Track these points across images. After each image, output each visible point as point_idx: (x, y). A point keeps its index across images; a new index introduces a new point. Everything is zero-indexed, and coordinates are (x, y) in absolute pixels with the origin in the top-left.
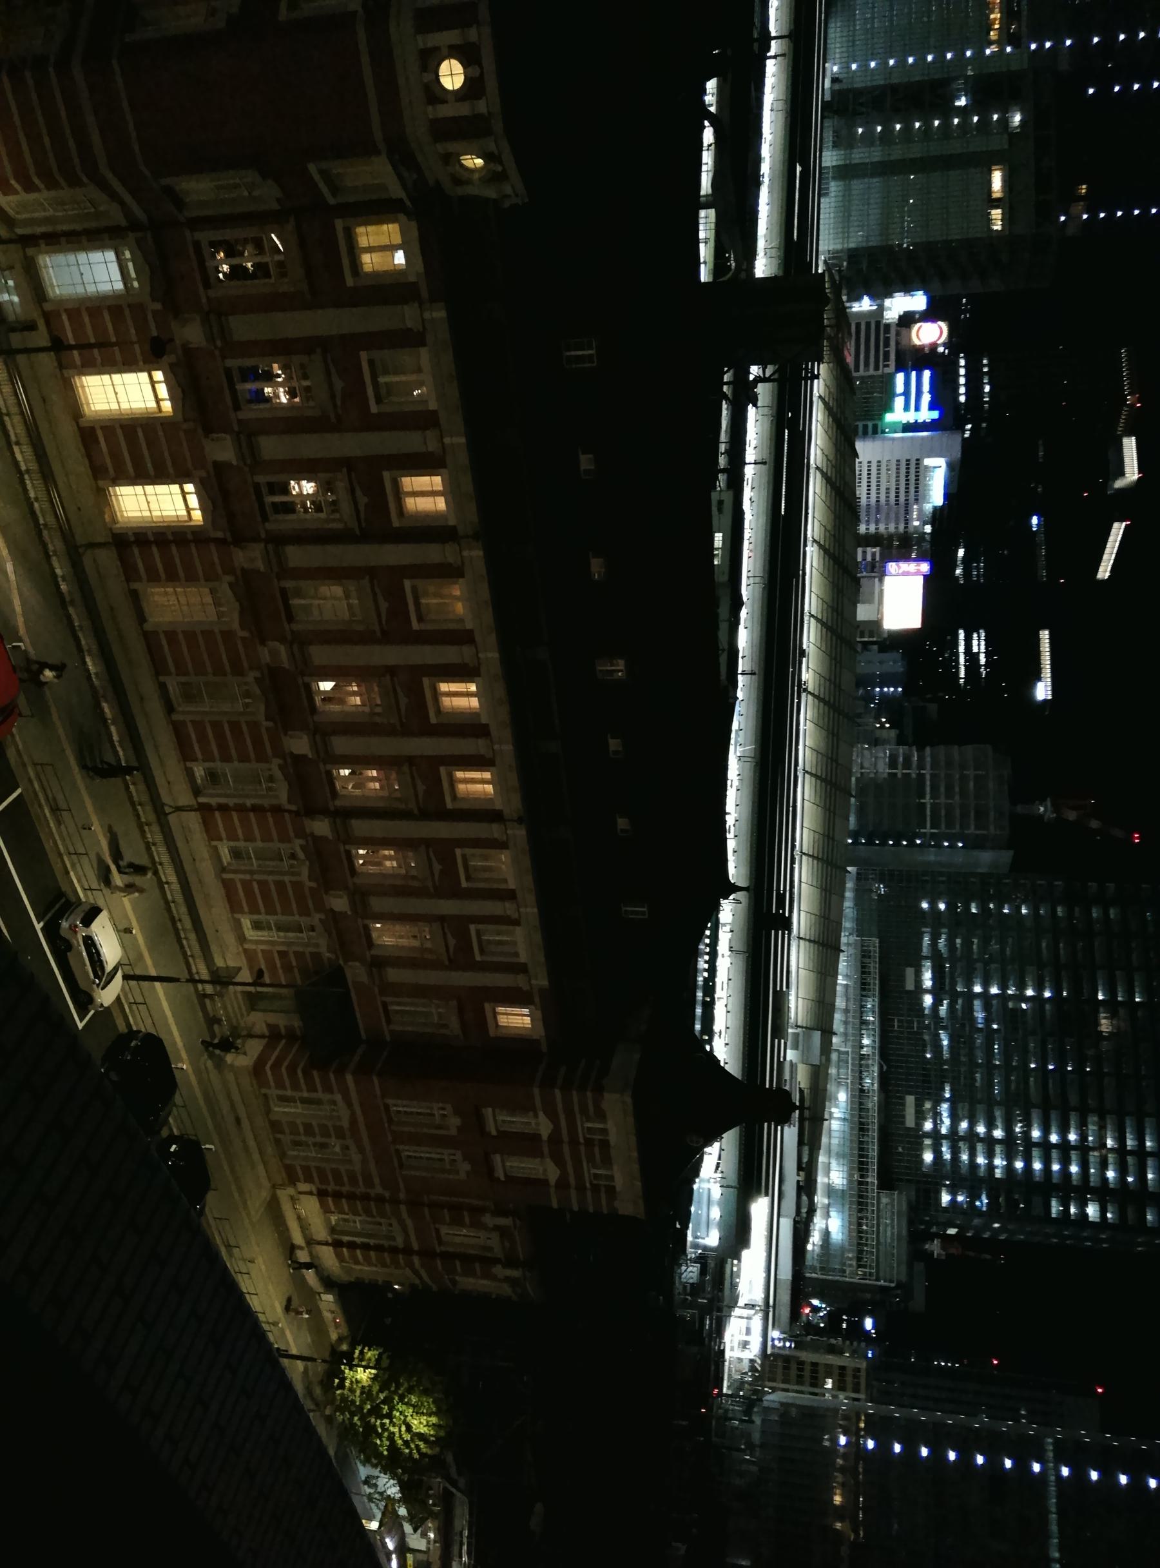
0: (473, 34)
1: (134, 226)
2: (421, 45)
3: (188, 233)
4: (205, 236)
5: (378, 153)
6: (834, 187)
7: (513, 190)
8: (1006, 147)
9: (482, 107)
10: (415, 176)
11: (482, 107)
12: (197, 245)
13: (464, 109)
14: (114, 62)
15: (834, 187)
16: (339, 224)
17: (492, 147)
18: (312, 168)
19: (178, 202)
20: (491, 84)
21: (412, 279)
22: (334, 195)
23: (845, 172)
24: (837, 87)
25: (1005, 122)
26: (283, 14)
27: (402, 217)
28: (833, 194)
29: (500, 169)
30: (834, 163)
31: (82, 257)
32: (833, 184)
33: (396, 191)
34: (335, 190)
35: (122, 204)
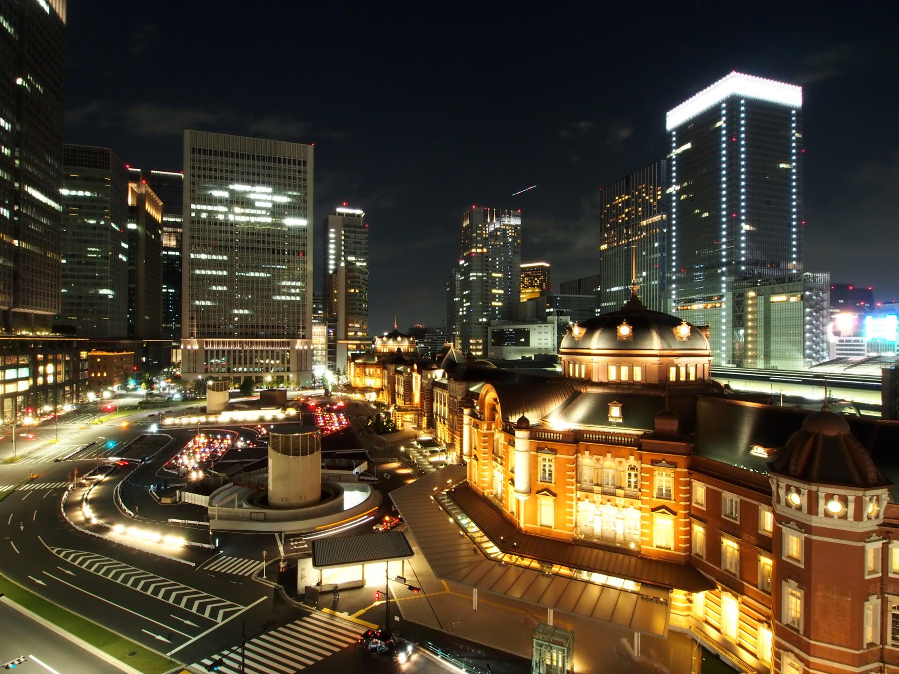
0: (821, 495)
2: (823, 516)
3: (886, 647)
6: (773, 363)
8: (763, 297)
9: (851, 498)
10: (874, 534)
11: (851, 498)
13: (852, 507)
14: (812, 642)
15: (773, 363)
16: (891, 575)
17: (868, 498)
18: (867, 577)
19: (871, 645)
20: (842, 491)
22: (877, 573)
23: (767, 356)
24: (731, 362)
25: (752, 298)
26: (802, 566)
27: (890, 546)
28: (777, 365)
30: (763, 363)
32: (772, 364)
33: (879, 545)
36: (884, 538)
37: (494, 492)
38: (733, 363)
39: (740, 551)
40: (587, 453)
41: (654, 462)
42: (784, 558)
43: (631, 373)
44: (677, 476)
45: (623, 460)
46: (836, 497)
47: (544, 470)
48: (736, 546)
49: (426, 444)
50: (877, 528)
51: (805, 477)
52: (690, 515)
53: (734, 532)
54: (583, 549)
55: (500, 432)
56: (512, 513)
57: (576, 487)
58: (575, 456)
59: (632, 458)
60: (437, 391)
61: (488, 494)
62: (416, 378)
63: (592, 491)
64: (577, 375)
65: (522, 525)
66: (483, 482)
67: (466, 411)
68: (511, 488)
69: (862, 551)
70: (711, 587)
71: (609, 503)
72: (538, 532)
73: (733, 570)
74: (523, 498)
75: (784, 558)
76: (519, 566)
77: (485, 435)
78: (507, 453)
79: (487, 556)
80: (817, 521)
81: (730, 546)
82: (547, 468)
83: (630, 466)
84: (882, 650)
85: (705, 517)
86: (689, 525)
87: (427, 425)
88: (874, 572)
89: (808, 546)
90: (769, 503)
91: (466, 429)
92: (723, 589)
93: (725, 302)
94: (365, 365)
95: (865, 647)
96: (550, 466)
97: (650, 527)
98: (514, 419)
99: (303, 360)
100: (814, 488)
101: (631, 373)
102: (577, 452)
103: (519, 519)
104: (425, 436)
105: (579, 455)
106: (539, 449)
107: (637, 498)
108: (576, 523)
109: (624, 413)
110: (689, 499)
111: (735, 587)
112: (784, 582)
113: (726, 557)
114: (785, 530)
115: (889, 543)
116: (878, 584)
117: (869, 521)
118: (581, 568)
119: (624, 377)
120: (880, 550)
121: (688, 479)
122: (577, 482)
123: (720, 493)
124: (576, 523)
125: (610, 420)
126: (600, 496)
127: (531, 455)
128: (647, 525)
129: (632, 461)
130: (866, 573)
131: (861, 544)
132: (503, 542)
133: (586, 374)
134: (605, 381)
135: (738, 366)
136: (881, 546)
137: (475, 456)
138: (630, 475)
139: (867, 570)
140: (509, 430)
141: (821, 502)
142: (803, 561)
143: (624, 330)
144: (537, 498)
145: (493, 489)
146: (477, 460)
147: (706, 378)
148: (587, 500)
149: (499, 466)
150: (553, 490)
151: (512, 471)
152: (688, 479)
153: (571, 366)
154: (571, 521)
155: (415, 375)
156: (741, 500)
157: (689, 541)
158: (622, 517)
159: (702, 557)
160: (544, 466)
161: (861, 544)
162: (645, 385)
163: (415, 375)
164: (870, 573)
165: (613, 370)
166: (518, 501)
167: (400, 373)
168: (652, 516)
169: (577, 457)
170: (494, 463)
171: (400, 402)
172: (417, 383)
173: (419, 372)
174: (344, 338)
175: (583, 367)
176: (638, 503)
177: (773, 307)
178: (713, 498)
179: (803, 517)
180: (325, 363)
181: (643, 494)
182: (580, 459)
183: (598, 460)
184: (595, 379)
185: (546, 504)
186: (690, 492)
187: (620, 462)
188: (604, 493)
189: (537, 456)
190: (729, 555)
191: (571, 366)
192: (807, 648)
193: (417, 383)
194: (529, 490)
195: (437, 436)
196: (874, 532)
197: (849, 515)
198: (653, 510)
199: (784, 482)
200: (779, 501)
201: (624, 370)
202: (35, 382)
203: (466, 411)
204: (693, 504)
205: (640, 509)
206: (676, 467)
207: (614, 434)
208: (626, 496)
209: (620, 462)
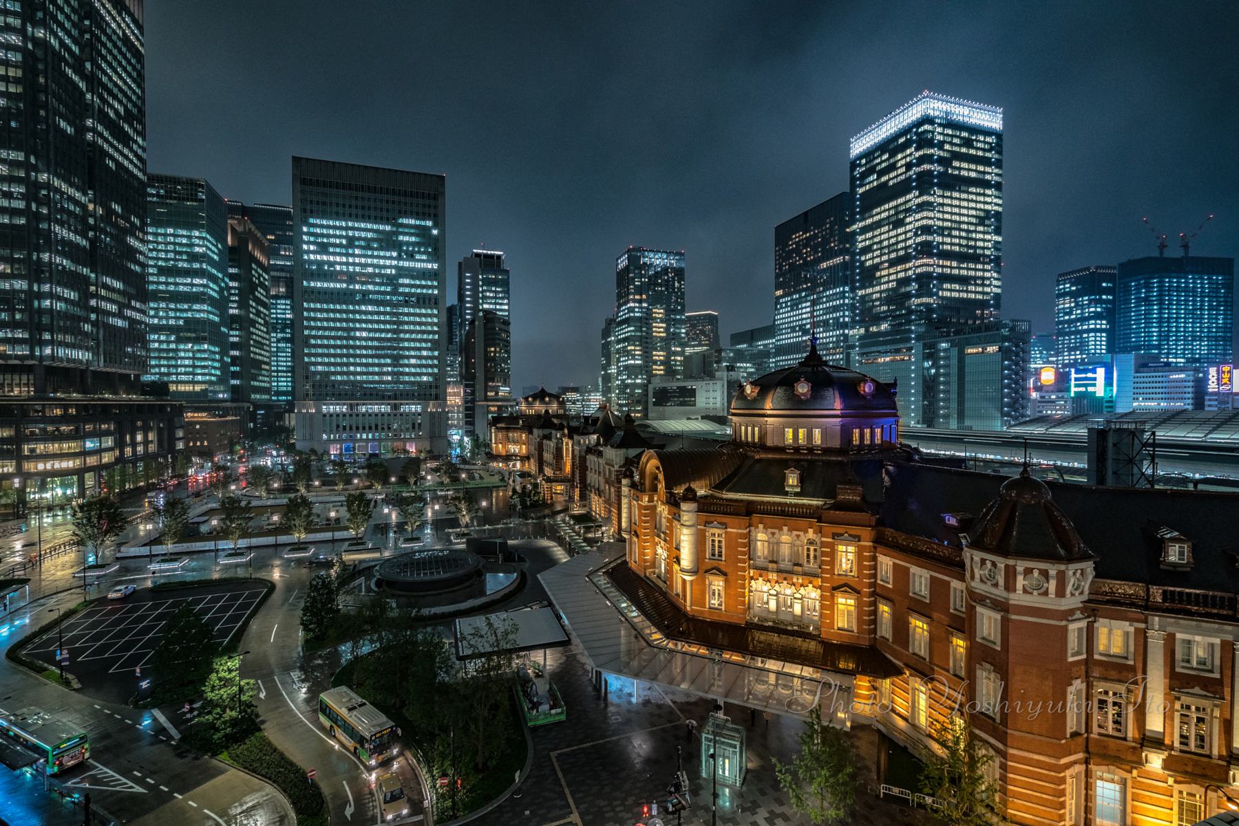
0: (1020, 569)
1: (1087, 762)
4: (1096, 729)
6: (967, 423)
7: (1089, 566)
11: (1052, 572)
12: (1100, 734)
16: (1096, 657)
17: (1071, 573)
18: (1070, 659)
19: (1075, 735)
20: (1043, 566)
21: (1132, 629)
22: (1082, 654)
23: (961, 416)
25: (945, 350)
27: (1096, 625)
31: (1099, 801)
34: (1078, 653)
36: (1089, 617)
37: (657, 571)
38: (923, 423)
39: (930, 632)
40: (761, 526)
41: (834, 536)
42: (978, 640)
43: (810, 436)
45: (801, 533)
46: (1036, 573)
48: (925, 627)
49: (579, 519)
50: (1081, 605)
51: (1002, 550)
52: (873, 594)
53: (922, 610)
54: (755, 632)
55: (663, 503)
56: (678, 595)
59: (811, 531)
60: (591, 459)
61: (650, 573)
62: (567, 444)
63: (766, 569)
64: (750, 439)
65: (688, 609)
66: (645, 561)
67: (624, 481)
68: (676, 567)
69: (1065, 629)
70: (898, 672)
71: (785, 582)
73: (922, 653)
74: (688, 578)
75: (978, 640)
76: (684, 653)
77: (646, 508)
78: (671, 528)
79: (649, 644)
80: (1018, 598)
81: (919, 626)
82: (717, 544)
84: (1087, 738)
85: (892, 596)
86: (874, 604)
87: (580, 497)
88: (1078, 653)
89: (1005, 622)
90: (962, 579)
91: (624, 501)
92: (911, 675)
93: (914, 355)
95: (1068, 736)
96: (720, 542)
97: (832, 607)
98: (679, 490)
100: (1011, 562)
101: (810, 436)
102: (750, 526)
103: (685, 601)
104: (577, 511)
105: (753, 528)
106: (707, 523)
107: (816, 576)
109: (802, 480)
110: (874, 576)
111: (925, 674)
112: (978, 666)
113: (914, 640)
114: (979, 609)
115: (1095, 622)
116: (1083, 667)
118: (754, 654)
119: (802, 440)
120: (1085, 630)
122: (750, 559)
123: (908, 569)
125: (787, 489)
126: (775, 575)
127: (698, 530)
128: (828, 603)
129: (811, 534)
130: (1069, 654)
131: (1064, 623)
132: (668, 627)
133: (759, 438)
134: (781, 445)
135: (929, 426)
137: (635, 532)
138: (808, 550)
139: (1070, 652)
140: (673, 502)
141: (1020, 579)
143: (803, 389)
144: (704, 579)
145: (655, 567)
146: (637, 536)
147: (893, 442)
148: (761, 579)
149: (662, 542)
150: (723, 569)
151: (679, 550)
153: (743, 428)
155: (565, 440)
156: (931, 576)
157: (874, 622)
158: (800, 596)
160: (713, 541)
161: (1064, 623)
162: (827, 451)
163: (565, 440)
164: (1073, 655)
165: (789, 433)
166: (684, 581)
167: (548, 437)
168: (833, 596)
169: (750, 531)
170: (657, 539)
171: (548, 472)
172: (567, 449)
173: (571, 437)
174: (483, 398)
175: (756, 429)
176: (819, 582)
177: (968, 360)
178: (901, 575)
179: (1000, 592)
180: (461, 428)
181: (824, 571)
182: (753, 534)
183: (773, 534)
184: (769, 443)
185: (718, 584)
186: (875, 568)
188: (779, 571)
189: (705, 530)
190: (917, 636)
191: (743, 428)
192: (1003, 738)
193: (567, 449)
194: (696, 570)
195: (591, 509)
196: (1078, 609)
197: (1050, 591)
198: (835, 589)
199: (978, 555)
200: (973, 577)
201: (802, 432)
202: (122, 452)
203: (624, 481)
204: (879, 582)
205: (820, 588)
206: (859, 541)
207: (791, 505)
208: (805, 574)
209: (798, 536)
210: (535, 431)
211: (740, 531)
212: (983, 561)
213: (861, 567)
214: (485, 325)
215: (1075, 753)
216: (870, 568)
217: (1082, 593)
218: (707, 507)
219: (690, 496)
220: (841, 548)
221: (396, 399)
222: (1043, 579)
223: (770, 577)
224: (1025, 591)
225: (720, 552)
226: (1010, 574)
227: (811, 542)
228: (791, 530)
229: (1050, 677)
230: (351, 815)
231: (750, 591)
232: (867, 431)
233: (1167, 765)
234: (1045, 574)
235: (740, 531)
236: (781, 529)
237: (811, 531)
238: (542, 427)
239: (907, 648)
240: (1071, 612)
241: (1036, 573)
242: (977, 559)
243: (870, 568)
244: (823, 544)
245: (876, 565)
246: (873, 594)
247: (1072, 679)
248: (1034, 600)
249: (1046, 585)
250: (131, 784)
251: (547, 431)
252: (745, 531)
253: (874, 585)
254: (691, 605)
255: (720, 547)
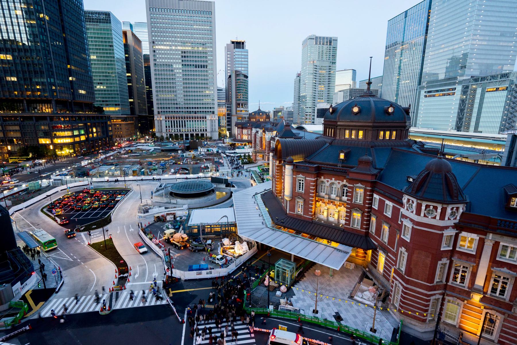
5: (443, 234)
16: (457, 249)
18: (442, 249)
29: (455, 208)
35: (437, 294)
44: (366, 191)
45: (341, 182)
46: (431, 207)
47: (300, 185)
50: (453, 225)
57: (316, 195)
58: (316, 179)
65: (288, 212)
66: (277, 190)
71: (332, 204)
72: (295, 216)
77: (278, 166)
80: (420, 219)
83: (344, 185)
86: (369, 216)
94: (242, 128)
96: (303, 183)
99: (214, 125)
105: (318, 178)
108: (315, 213)
110: (371, 204)
112: (400, 248)
117: (449, 221)
121: (371, 193)
122: (316, 192)
123: (385, 201)
124: (315, 213)
129: (345, 182)
135: (458, 131)
136: (455, 234)
138: (344, 190)
142: (409, 239)
148: (321, 202)
152: (371, 193)
154: (311, 212)
156: (393, 205)
157: (368, 225)
159: (373, 233)
168: (351, 211)
169: (317, 180)
177: (487, 95)
178: (382, 203)
180: (226, 127)
186: (371, 200)
187: (339, 183)
196: (451, 226)
202: (88, 136)
203: (271, 154)
204: (373, 206)
210: (253, 129)
211: (311, 179)
212: (409, 200)
213: (365, 199)
214: (236, 78)
215: (438, 290)
216: (370, 200)
217: (455, 219)
218: (297, 169)
219: (291, 163)
220: (358, 190)
221: (195, 113)
222: (434, 210)
223: (325, 201)
224: (425, 216)
225: (303, 188)
226: (419, 207)
227: (345, 186)
228: (336, 180)
229: (430, 256)
230: (137, 278)
231: (316, 207)
232: (388, 133)
233: (482, 300)
234: (436, 208)
235: (311, 179)
236: (331, 179)
237: (345, 181)
238: (256, 128)
239: (380, 237)
240: (447, 227)
241: (431, 207)
242: (406, 199)
243: (370, 200)
244: (349, 187)
245: (372, 199)
246: (368, 212)
247: (442, 258)
248: (429, 220)
249: (436, 214)
250: (69, 258)
251: (258, 129)
252: (314, 179)
253: (370, 208)
254: (290, 211)
255: (303, 186)
